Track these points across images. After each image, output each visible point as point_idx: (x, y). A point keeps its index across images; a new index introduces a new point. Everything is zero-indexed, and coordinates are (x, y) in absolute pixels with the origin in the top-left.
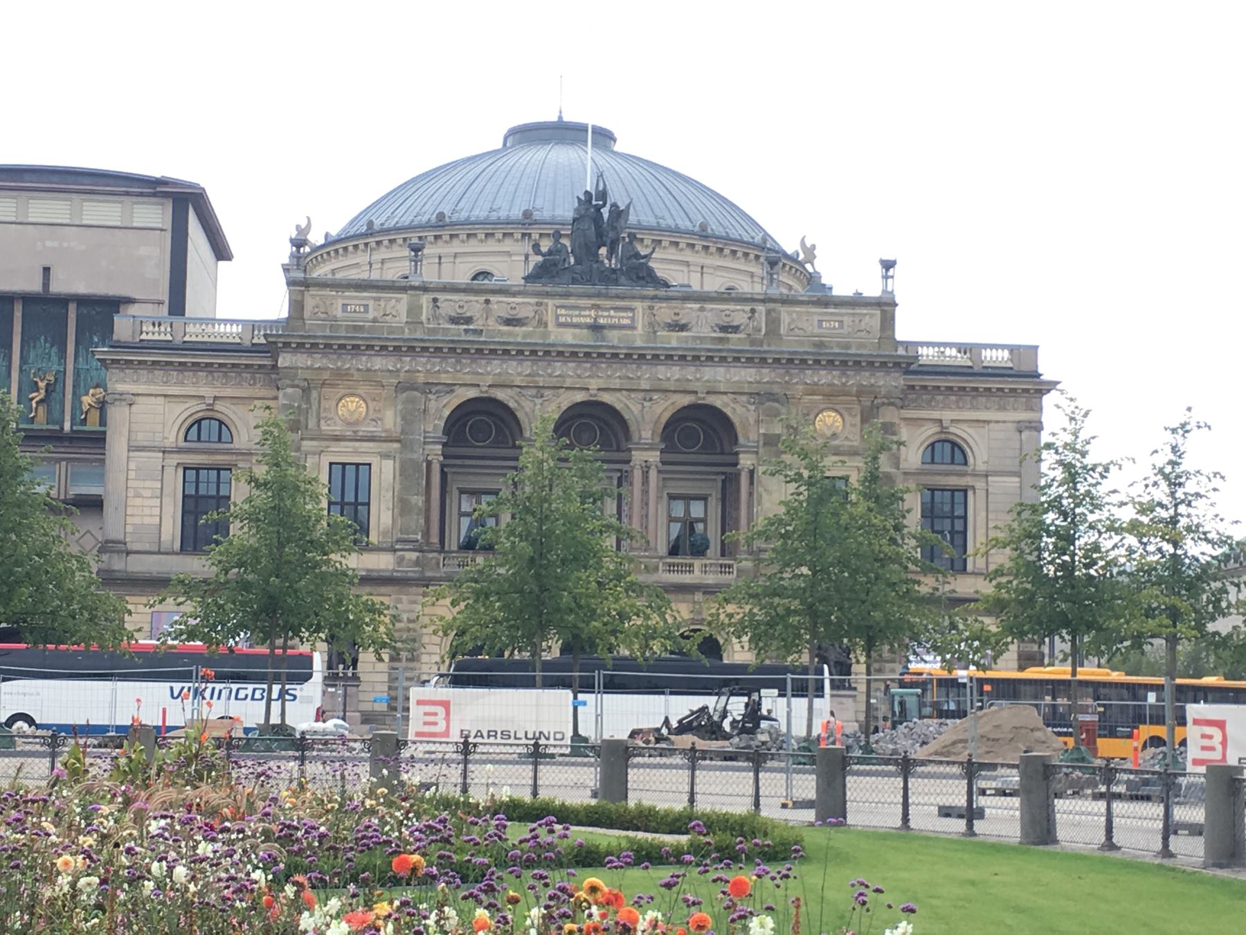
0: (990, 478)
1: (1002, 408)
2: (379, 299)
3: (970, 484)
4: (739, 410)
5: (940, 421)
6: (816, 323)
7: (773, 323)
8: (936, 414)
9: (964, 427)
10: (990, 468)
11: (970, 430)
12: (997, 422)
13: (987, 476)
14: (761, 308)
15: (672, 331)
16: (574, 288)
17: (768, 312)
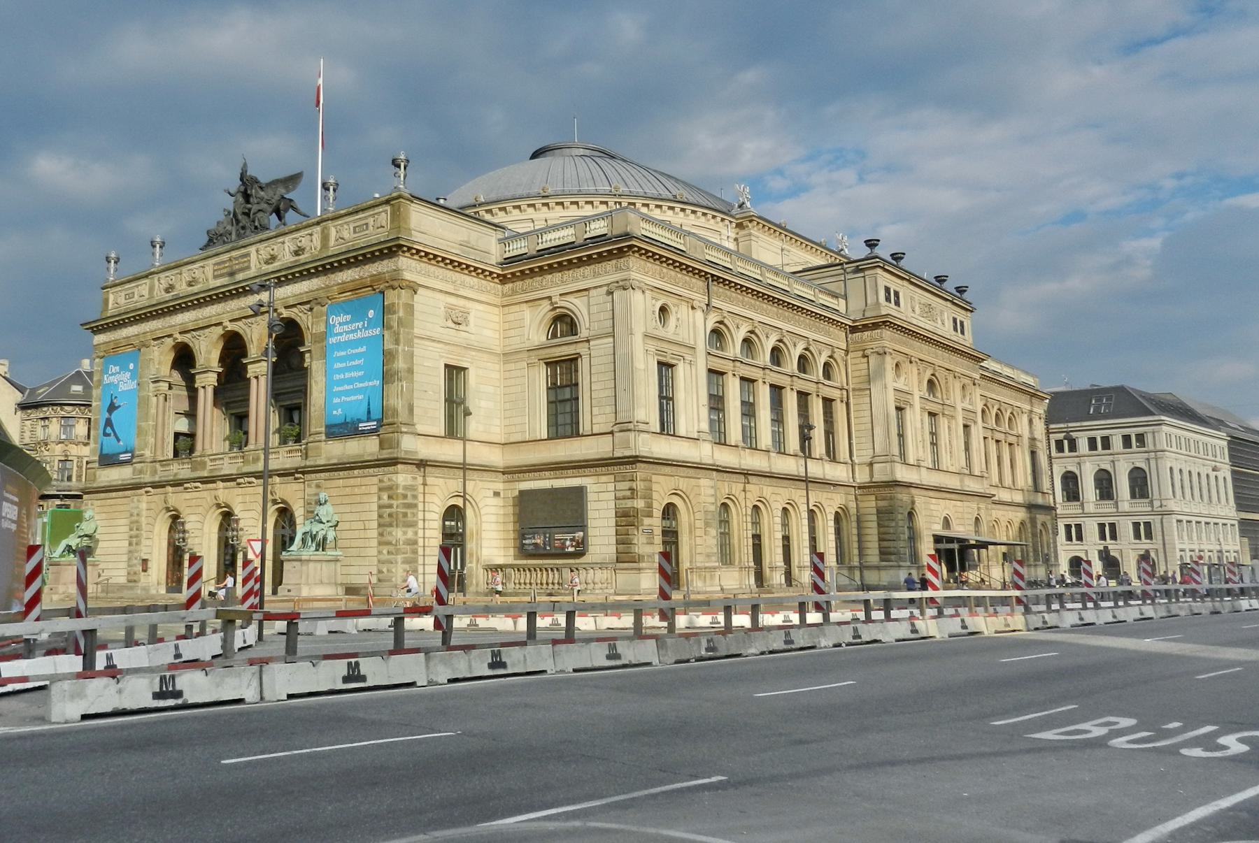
0: (591, 343)
1: (596, 275)
2: (137, 286)
3: (578, 351)
4: (304, 317)
5: (550, 298)
6: (352, 228)
7: (325, 238)
8: (546, 293)
9: (570, 298)
10: (592, 333)
11: (576, 301)
12: (595, 287)
13: (588, 341)
14: (318, 229)
15: (269, 264)
16: (220, 249)
17: (323, 232)
